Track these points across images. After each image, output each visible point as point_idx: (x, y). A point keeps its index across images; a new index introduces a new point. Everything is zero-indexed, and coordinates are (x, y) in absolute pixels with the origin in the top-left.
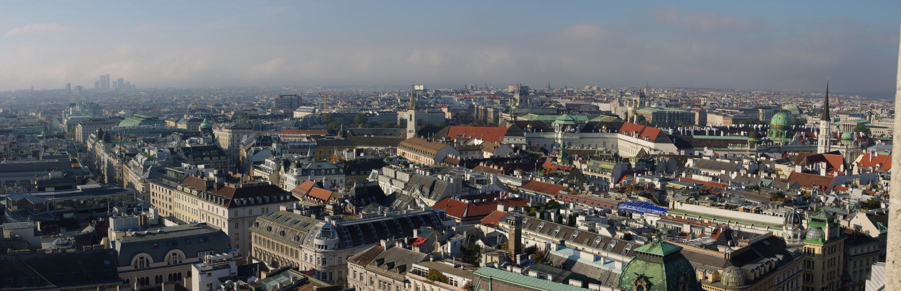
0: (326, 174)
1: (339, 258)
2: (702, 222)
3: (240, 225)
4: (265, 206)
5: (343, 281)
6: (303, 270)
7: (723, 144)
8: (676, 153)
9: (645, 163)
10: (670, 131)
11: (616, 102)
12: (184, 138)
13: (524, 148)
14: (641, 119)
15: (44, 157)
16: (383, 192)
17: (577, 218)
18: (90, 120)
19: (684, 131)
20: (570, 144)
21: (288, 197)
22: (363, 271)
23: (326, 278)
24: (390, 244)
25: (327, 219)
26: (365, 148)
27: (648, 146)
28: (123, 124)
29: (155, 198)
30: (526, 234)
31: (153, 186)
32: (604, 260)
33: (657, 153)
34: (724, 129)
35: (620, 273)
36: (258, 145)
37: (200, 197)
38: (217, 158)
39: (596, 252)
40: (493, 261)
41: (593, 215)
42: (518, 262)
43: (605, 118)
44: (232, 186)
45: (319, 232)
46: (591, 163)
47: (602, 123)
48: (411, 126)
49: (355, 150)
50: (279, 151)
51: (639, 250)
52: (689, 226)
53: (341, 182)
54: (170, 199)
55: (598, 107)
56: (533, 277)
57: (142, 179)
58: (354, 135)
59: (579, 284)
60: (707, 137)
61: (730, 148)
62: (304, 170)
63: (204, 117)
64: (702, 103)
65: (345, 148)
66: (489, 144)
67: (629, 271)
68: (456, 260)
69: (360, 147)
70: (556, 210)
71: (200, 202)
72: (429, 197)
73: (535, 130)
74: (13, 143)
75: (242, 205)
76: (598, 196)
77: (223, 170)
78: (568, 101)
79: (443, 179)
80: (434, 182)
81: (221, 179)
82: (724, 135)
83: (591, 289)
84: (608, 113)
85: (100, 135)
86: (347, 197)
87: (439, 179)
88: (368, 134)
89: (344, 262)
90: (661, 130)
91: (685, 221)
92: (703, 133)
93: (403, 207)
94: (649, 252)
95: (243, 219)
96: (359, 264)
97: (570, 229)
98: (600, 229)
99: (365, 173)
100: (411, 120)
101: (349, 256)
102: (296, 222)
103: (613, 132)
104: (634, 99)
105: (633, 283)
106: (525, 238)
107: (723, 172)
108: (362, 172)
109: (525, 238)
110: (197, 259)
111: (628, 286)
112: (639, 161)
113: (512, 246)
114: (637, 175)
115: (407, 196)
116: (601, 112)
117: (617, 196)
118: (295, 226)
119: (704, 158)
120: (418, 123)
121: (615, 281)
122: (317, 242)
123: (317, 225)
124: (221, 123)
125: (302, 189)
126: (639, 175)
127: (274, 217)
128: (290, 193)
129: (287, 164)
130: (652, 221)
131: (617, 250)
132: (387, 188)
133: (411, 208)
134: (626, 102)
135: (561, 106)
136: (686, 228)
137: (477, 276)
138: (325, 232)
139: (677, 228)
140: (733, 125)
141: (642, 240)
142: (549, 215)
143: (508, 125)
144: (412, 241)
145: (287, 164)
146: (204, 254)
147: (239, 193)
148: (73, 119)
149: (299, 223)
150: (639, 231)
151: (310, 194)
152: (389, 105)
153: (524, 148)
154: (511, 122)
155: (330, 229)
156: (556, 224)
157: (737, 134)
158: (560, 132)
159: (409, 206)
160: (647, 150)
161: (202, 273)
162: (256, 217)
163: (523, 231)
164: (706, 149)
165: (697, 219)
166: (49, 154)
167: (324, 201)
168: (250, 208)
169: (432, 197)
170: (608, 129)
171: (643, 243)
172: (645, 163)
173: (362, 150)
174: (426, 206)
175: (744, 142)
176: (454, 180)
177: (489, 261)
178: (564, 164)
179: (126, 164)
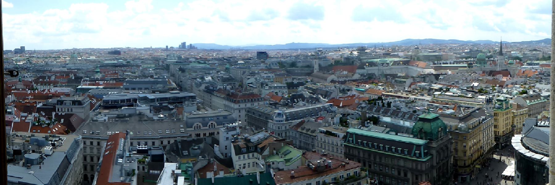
3: (241, 111)
12: (218, 72)
18: (177, 62)
21: (263, 99)
23: (280, 135)
36: (249, 76)
46: (396, 79)
48: (316, 67)
49: (292, 78)
51: (420, 116)
53: (286, 92)
66: (350, 74)
70: (381, 101)
73: (370, 66)
75: (242, 102)
77: (234, 87)
88: (297, 71)
93: (313, 103)
95: (242, 109)
99: (296, 88)
108: (295, 88)
120: (320, 65)
123: (275, 111)
124: (233, 65)
131: (410, 118)
132: (307, 94)
137: (348, 132)
143: (358, 65)
154: (359, 63)
159: (316, 102)
166: (157, 77)
169: (326, 98)
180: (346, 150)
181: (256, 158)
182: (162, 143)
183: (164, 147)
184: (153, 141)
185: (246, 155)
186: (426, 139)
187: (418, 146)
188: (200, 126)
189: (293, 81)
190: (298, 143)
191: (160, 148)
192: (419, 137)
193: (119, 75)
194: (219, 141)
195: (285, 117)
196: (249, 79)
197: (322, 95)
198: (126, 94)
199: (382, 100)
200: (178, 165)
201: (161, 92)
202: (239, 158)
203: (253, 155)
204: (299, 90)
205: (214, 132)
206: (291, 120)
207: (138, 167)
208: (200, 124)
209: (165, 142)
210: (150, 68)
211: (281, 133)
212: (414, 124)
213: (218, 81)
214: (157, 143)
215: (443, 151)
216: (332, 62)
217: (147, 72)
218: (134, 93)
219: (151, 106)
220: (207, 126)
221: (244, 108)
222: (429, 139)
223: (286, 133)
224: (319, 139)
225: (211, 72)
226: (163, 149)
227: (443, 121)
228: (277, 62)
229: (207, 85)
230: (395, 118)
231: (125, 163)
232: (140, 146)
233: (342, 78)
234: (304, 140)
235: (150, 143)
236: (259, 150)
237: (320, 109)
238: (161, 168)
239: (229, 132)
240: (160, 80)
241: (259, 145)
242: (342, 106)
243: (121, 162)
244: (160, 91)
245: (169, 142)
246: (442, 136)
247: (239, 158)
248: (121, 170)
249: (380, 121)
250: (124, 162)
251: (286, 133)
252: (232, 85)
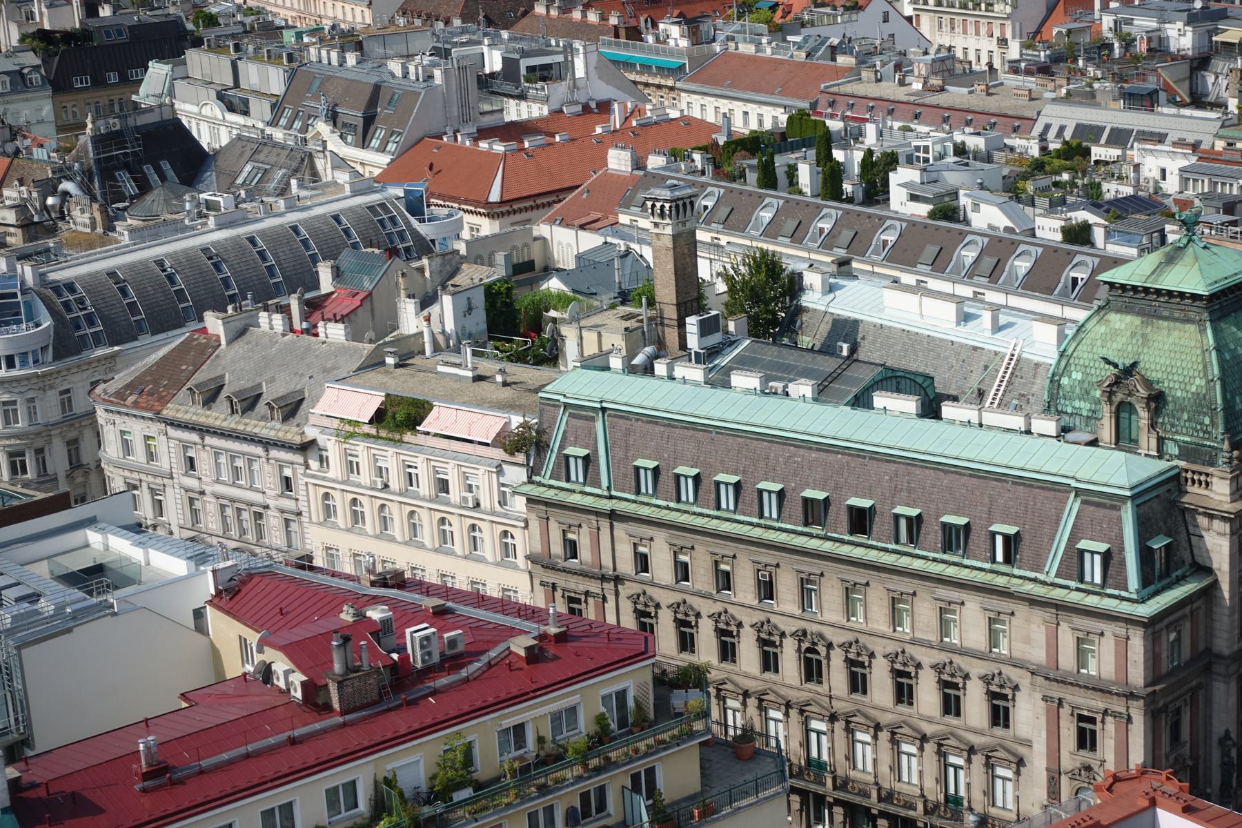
1: (62, 393)
5: (86, 474)
16: (196, 144)
17: (891, 175)
22: (154, 428)
23: (24, 471)
24: (238, 325)
30: (715, 246)
32: (995, 320)
35: (1053, 362)
39: (965, 291)
40: (606, 347)
41: (951, 159)
42: (693, 342)
51: (1117, 275)
56: (747, 391)
59: (908, 404)
67: (1084, 353)
68: (475, 354)
72: (364, 143)
76: (965, 90)
79: (406, 74)
80: (377, 88)
83: (952, 422)
86: (63, 173)
87: (393, 75)
89: (80, 404)
94: (1155, 281)
96: (136, 405)
97: (870, 216)
98: (976, 208)
101: (94, 384)
105: (1098, 393)
106: (711, 260)
108: (113, 78)
109: (711, 260)
111: (1082, 404)
113: (666, 293)
115: (283, 147)
117: (1033, 86)
121: (1035, 389)
130: (1163, 171)
133: (301, 186)
137: (554, 404)
141: (1128, 242)
142: (792, 172)
144: (314, 307)
150: (1118, 210)
155: (14, 295)
156: (819, 201)
159: (294, 182)
163: (702, 236)
169: (375, 143)
171: (1134, 252)
176: (446, 73)
177: (591, 349)
180: (546, 534)
186: (1161, 455)
189: (93, 23)
190: (175, 513)
192: (1106, 432)
195: (47, 323)
197: (333, 118)
199: (825, 142)
204: (143, 90)
206: (98, 343)
212: (1070, 331)
222: (1187, 452)
223: (73, 446)
224: (336, 469)
230: (919, 289)
234: (217, 481)
242: (502, 203)
249: (806, 310)
251: (73, 446)
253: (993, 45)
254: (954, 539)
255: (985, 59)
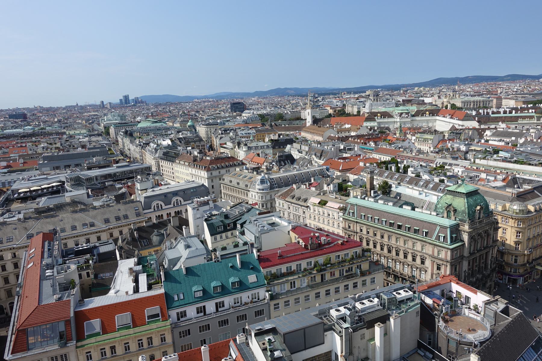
0: (261, 148)
2: (495, 171)
4: (228, 169)
6: (251, 203)
7: (515, 119)
8: (477, 127)
9: (455, 134)
10: (474, 113)
11: (436, 97)
12: (179, 132)
13: (376, 128)
14: (453, 106)
15: (89, 149)
19: (484, 112)
20: (405, 124)
22: (284, 202)
24: (298, 187)
25: (263, 175)
26: (283, 133)
27: (458, 123)
28: (140, 125)
29: (163, 169)
31: (161, 161)
32: (426, 195)
33: (464, 128)
34: (516, 110)
36: (222, 134)
37: (190, 166)
38: (198, 143)
39: (421, 189)
41: (419, 167)
42: (372, 195)
43: (429, 107)
44: (208, 158)
45: (259, 181)
46: (418, 135)
47: (426, 110)
49: (277, 134)
50: (234, 137)
51: (449, 189)
52: (485, 174)
54: (172, 168)
55: (423, 101)
56: (381, 204)
57: (154, 158)
58: (276, 125)
59: (410, 208)
60: (502, 115)
61: (519, 122)
62: (248, 147)
63: (189, 119)
64: (499, 92)
65: (271, 133)
66: (355, 127)
67: (442, 201)
69: (280, 133)
71: (190, 169)
72: (320, 159)
74: (66, 141)
75: (214, 169)
78: (404, 98)
80: (323, 150)
81: (202, 155)
82: (515, 113)
84: (431, 104)
85: (126, 133)
86: (273, 161)
90: (467, 113)
91: (482, 171)
92: (499, 113)
95: (216, 177)
98: (423, 175)
99: (283, 147)
100: (309, 115)
102: (245, 177)
103: (433, 115)
104: (448, 93)
107: (513, 138)
108: (282, 147)
110: (190, 202)
112: (451, 133)
113: (368, 186)
114: (449, 142)
116: (426, 104)
118: (245, 179)
119: (498, 129)
120: (313, 117)
122: (257, 187)
123: (257, 178)
124: (200, 122)
125: (248, 158)
126: (451, 142)
127: (233, 175)
128: (242, 161)
129: (239, 144)
131: (435, 188)
132: (296, 155)
134: (443, 96)
135: (399, 101)
136: (483, 176)
137: (348, 203)
138: (262, 182)
139: (477, 175)
140: (523, 106)
142: (391, 168)
143: (366, 115)
144: (310, 185)
145: (239, 144)
146: (194, 198)
147: (212, 162)
148: (107, 123)
149: (247, 177)
150: (450, 177)
151: (253, 160)
152: (296, 107)
153: (376, 128)
154: (368, 113)
157: (526, 111)
158: (399, 117)
160: (457, 127)
161: (194, 209)
162: (223, 175)
163: (375, 177)
164: (500, 123)
165: (492, 170)
167: (261, 164)
168: (219, 170)
170: (430, 114)
171: (452, 185)
172: (455, 134)
173: (281, 134)
174: (318, 164)
175: (531, 117)
177: (355, 195)
178: (400, 137)
179: (144, 150)
181: (236, 237)
182: (111, 235)
183: (116, 241)
184: (98, 234)
185: (224, 235)
187: (443, 227)
188: (161, 205)
189: (279, 138)
190: (286, 215)
191: (110, 242)
192: (445, 215)
193: (29, 149)
194: (188, 221)
195: (269, 184)
196: (221, 138)
197: (315, 155)
198: (45, 176)
200: (136, 260)
201: (100, 167)
202: (215, 239)
203: (232, 234)
205: (181, 211)
206: (276, 188)
207: (80, 276)
208: (160, 203)
209: (116, 234)
210: (79, 134)
211: (266, 204)
212: (439, 198)
213: (180, 144)
214: (104, 237)
215: (482, 237)
216: (330, 113)
217: (74, 141)
218: (58, 174)
219: (87, 189)
220: (171, 204)
221: (218, 176)
222: (460, 220)
223: (271, 203)
224: (312, 211)
225: (169, 132)
226: (113, 244)
227: (485, 197)
228: (258, 114)
229: (165, 151)
230: (412, 188)
231: (58, 274)
232: (80, 246)
233: (343, 133)
235: (93, 239)
236: (239, 226)
237: (314, 174)
238: (114, 267)
239: (200, 208)
240: (98, 150)
241: (238, 220)
243: (51, 274)
244: (99, 166)
245: (121, 233)
246: (481, 217)
247: (215, 239)
248: (53, 286)
250: (56, 274)
251: (271, 203)
252: (201, 148)
253: (428, 148)
254: (416, 231)
255: (426, 150)
